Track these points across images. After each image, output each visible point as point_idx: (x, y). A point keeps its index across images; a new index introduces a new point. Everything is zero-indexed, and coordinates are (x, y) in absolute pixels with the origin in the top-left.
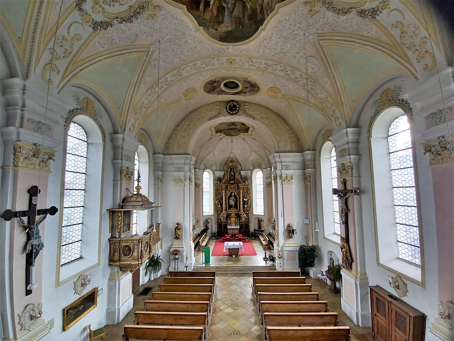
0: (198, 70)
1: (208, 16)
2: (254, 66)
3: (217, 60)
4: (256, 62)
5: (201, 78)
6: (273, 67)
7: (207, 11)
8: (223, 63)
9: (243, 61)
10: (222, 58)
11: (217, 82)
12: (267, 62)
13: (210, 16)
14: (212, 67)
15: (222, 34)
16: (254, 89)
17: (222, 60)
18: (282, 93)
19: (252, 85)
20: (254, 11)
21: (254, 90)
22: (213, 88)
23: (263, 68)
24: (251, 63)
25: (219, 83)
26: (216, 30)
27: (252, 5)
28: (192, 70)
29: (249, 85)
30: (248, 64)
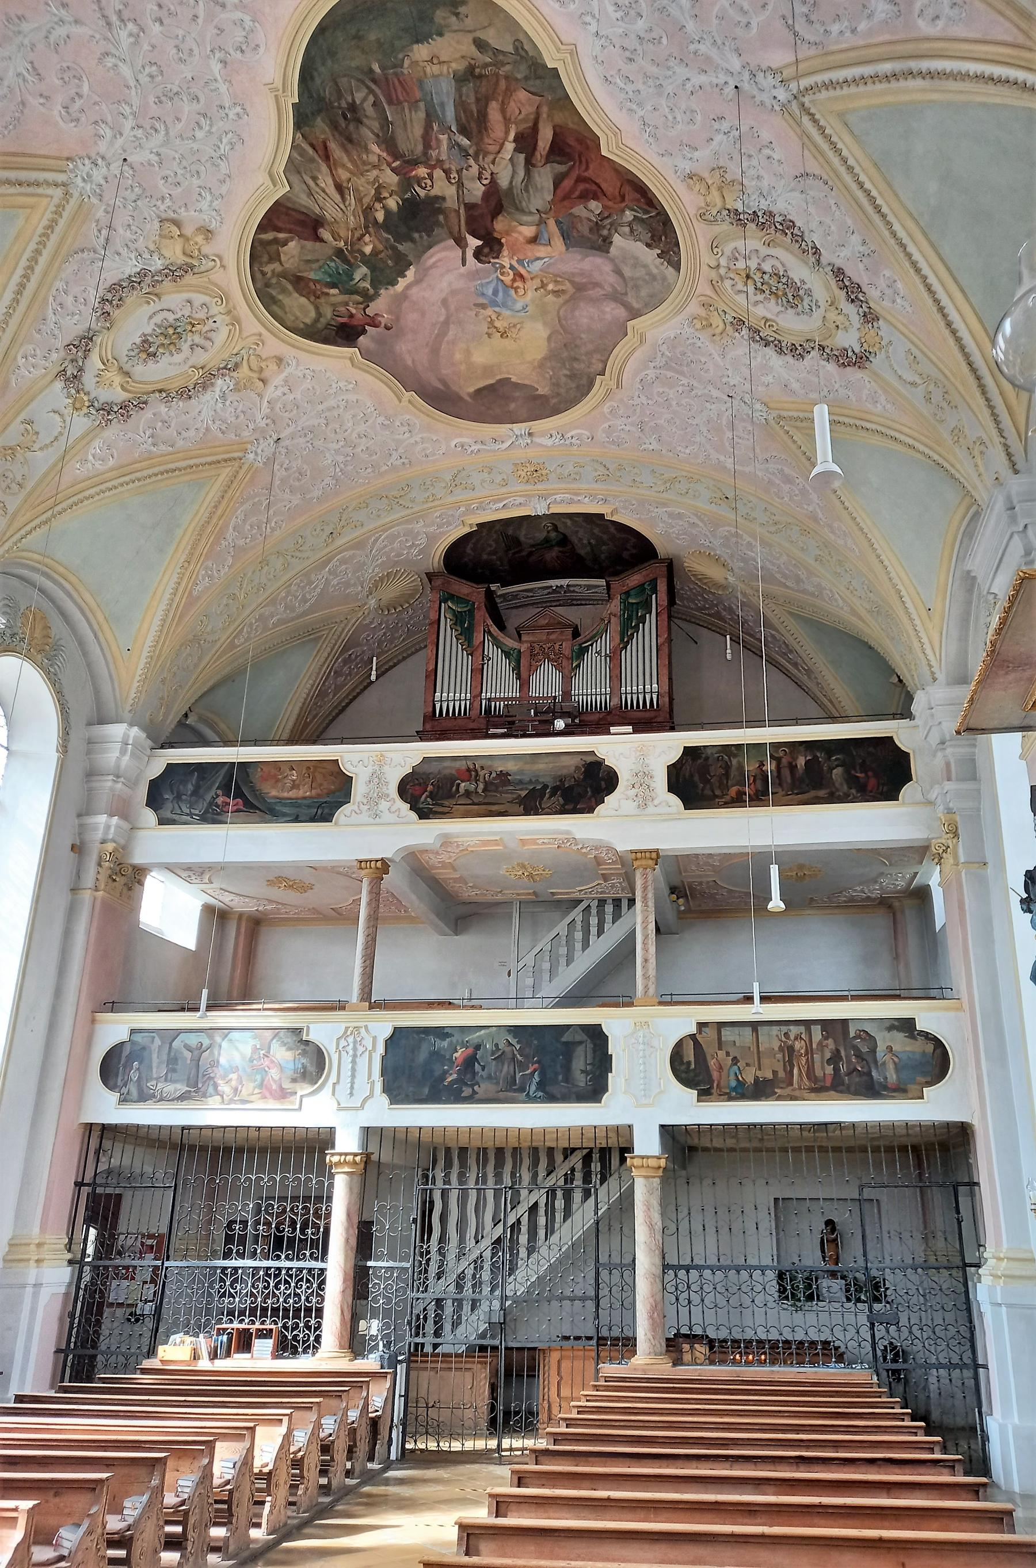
1: (523, 104)
7: (524, 120)
13: (512, 104)
20: (350, 140)
26: (480, 44)
27: (365, 157)
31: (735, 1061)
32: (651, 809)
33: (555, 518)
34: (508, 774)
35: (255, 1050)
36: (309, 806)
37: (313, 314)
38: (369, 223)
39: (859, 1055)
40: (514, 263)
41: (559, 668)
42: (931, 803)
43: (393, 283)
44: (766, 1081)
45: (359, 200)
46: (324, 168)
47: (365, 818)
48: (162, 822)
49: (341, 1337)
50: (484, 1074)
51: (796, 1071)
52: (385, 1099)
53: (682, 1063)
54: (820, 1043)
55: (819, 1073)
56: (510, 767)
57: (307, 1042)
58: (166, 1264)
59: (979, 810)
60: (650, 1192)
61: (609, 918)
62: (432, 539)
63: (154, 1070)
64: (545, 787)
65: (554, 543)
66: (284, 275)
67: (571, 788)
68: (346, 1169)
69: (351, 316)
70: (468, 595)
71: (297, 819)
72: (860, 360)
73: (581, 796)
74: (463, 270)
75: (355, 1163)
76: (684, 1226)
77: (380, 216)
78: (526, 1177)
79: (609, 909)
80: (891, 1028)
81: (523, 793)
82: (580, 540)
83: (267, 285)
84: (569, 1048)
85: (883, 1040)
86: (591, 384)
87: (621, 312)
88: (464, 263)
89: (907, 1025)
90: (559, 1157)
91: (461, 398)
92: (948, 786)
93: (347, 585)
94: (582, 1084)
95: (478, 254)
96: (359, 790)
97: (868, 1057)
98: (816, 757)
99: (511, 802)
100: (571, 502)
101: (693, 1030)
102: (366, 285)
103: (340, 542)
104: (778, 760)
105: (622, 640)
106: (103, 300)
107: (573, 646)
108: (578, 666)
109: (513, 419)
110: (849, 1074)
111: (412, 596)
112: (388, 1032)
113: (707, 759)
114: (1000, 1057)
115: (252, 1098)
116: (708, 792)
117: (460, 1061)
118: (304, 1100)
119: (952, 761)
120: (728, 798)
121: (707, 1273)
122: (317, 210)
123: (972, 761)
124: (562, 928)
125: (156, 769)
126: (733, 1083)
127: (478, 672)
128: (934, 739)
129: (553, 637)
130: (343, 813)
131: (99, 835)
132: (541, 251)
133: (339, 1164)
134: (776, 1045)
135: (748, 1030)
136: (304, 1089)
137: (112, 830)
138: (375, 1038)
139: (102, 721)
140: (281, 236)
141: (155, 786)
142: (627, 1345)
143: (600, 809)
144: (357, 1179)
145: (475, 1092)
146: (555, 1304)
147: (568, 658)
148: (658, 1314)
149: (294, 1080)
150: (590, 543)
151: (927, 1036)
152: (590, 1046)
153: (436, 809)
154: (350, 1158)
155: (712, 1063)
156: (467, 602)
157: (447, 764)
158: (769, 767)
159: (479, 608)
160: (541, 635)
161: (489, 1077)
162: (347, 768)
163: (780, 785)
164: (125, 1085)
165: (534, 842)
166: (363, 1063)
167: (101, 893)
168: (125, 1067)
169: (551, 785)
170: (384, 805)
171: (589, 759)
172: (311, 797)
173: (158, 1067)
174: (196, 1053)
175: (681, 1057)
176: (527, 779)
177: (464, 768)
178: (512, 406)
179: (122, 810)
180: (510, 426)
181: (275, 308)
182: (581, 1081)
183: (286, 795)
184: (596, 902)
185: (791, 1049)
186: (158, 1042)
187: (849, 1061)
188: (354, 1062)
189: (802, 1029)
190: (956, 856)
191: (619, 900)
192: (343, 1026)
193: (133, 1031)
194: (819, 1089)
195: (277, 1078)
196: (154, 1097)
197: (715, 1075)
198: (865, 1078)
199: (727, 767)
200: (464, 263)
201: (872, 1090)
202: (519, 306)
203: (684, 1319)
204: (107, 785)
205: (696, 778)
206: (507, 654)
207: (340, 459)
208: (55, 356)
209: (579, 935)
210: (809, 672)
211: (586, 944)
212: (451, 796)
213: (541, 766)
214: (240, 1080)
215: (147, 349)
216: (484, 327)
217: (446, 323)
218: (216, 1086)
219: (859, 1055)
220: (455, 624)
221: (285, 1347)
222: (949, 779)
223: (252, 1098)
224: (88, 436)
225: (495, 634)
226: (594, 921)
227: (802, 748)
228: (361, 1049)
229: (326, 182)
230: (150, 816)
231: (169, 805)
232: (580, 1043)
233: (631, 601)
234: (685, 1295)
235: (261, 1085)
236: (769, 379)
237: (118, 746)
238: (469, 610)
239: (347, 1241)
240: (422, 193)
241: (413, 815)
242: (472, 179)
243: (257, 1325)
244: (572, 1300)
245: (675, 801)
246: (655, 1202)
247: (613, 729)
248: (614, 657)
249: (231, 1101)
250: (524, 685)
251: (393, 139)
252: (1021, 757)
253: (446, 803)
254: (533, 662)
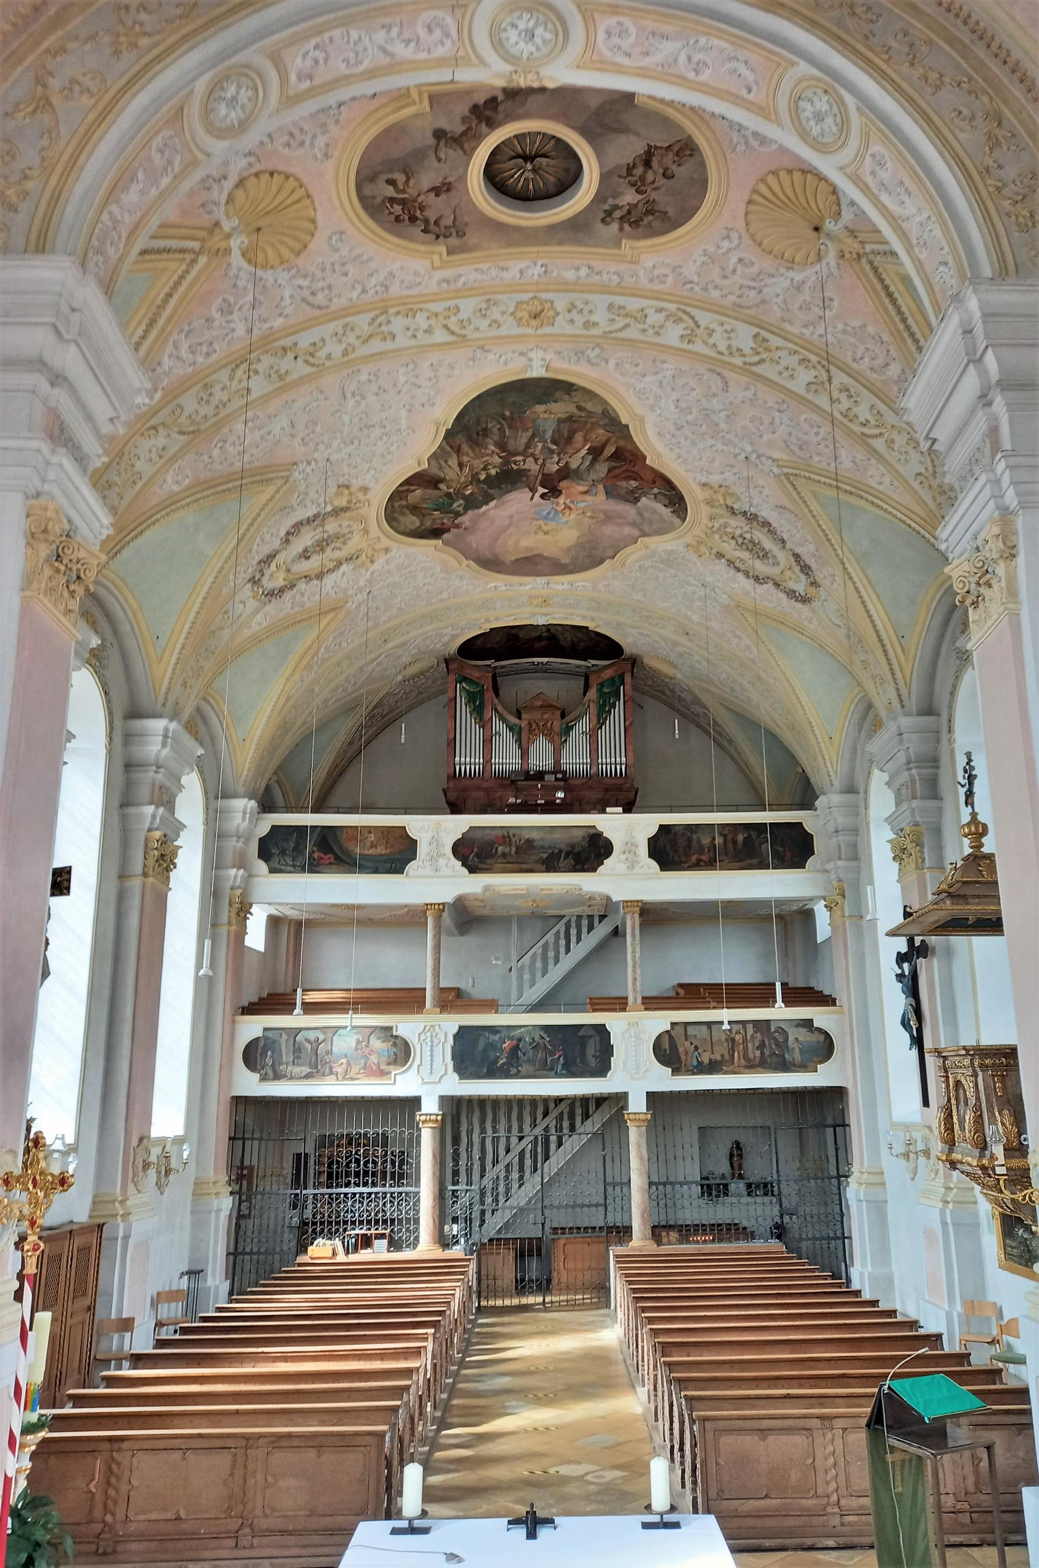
0: (684, 312)
2: (436, 315)
3: (595, 324)
4: (428, 331)
5: (690, 271)
6: (358, 337)
8: (569, 311)
9: (484, 324)
10: (569, 330)
11: (618, 214)
12: (389, 345)
14: (620, 300)
15: (566, 397)
16: (390, 191)
17: (572, 321)
18: (236, 259)
19: (413, 219)
21: (391, 182)
22: (650, 176)
23: (392, 319)
24: (453, 323)
25: (607, 207)
28: (711, 326)
29: (431, 215)
30: (463, 315)
31: (696, 1048)
32: (637, 870)
33: (548, 627)
34: (533, 841)
35: (358, 1042)
36: (385, 862)
37: (418, 524)
38: (474, 479)
39: (777, 1044)
40: (568, 502)
41: (552, 741)
42: (826, 871)
43: (479, 507)
44: (716, 1062)
45: (471, 469)
46: (455, 456)
47: (428, 871)
48: (272, 871)
49: (434, 1237)
50: (525, 1058)
51: (736, 1054)
52: (456, 1076)
53: (660, 1050)
54: (752, 1036)
55: (751, 1056)
56: (535, 835)
57: (397, 1037)
58: (304, 1192)
59: (858, 879)
60: (640, 1136)
61: (585, 929)
62: (454, 637)
63: (284, 1057)
64: (561, 851)
66: (407, 507)
67: (578, 852)
68: (431, 1125)
69: (443, 524)
70: (478, 678)
71: (376, 871)
72: (805, 600)
73: (588, 859)
74: (529, 503)
75: (437, 1120)
76: (662, 1157)
77: (482, 477)
78: (527, 1120)
79: (585, 923)
80: (797, 1026)
81: (545, 856)
83: (393, 512)
84: (584, 1041)
85: (793, 1034)
86: (602, 561)
87: (635, 532)
88: (532, 499)
89: (808, 1024)
90: (552, 1106)
91: (503, 562)
92: (840, 863)
93: (386, 670)
94: (593, 1065)
95: (543, 496)
96: (422, 850)
97: (784, 1045)
98: (750, 836)
99: (536, 862)
100: (567, 618)
101: (669, 1028)
102: (461, 509)
103: (390, 645)
104: (725, 836)
105: (599, 721)
106: (288, 533)
108: (566, 741)
109: (537, 574)
110: (770, 1056)
111: (428, 671)
112: (456, 1030)
113: (675, 834)
114: (867, 1046)
115: (358, 1076)
116: (676, 859)
117: (507, 1050)
118: (398, 1077)
119: (842, 844)
120: (690, 864)
121: (677, 1187)
122: (442, 475)
123: (855, 846)
124: (550, 937)
125: (263, 829)
126: (695, 1063)
127: (488, 742)
128: (831, 827)
129: (545, 716)
130: (411, 867)
131: (230, 883)
132: (588, 498)
133: (423, 1122)
134: (723, 1037)
135: (705, 1027)
136: (395, 1071)
137: (239, 879)
138: (446, 1034)
139: (226, 796)
140: (413, 488)
141: (262, 841)
142: (623, 1232)
143: (601, 869)
144: (438, 1131)
145: (519, 1071)
146: (578, 1209)
148: (645, 1214)
149: (389, 1064)
151: (820, 1030)
152: (598, 1039)
153: (484, 866)
154: (433, 1117)
155: (681, 1050)
156: (477, 684)
157: (487, 832)
158: (719, 840)
159: (487, 690)
160: (537, 715)
161: (529, 1061)
162: (413, 834)
163: (726, 854)
164: (263, 1068)
165: (551, 889)
166: (438, 1050)
167: (234, 927)
168: (261, 1055)
169: (565, 850)
170: (442, 862)
171: (592, 831)
172: (386, 855)
173: (287, 1056)
174: (314, 1045)
175: (660, 1046)
176: (547, 845)
177: (500, 835)
178: (539, 567)
179: (241, 863)
180: (534, 578)
181: (394, 524)
182: (592, 1062)
183: (366, 852)
184: (574, 919)
185: (733, 1040)
186: (284, 1037)
187: (771, 1047)
188: (432, 1050)
189: (741, 1026)
190: (843, 910)
191: (592, 916)
192: (422, 1025)
193: (265, 1029)
194: (751, 1066)
195: (376, 1062)
196: (285, 1076)
197: (683, 1057)
198: (781, 1059)
199: (690, 840)
200: (532, 499)
201: (784, 1066)
202: (564, 520)
203: (663, 1217)
204: (233, 844)
205: (668, 848)
206: (511, 729)
207: (407, 598)
208: (250, 570)
209: (562, 942)
210: (730, 741)
211: (568, 950)
212: (491, 856)
213: (557, 836)
214: (349, 1064)
215: (305, 555)
216: (534, 529)
217: (509, 525)
218: (331, 1068)
219: (777, 1044)
220: (469, 701)
221: (394, 1244)
222: (840, 859)
223: (358, 1076)
224: (256, 612)
226: (573, 932)
227: (741, 828)
228: (436, 1041)
229: (453, 462)
230: (262, 867)
231: (276, 859)
232: (591, 1037)
233: (606, 690)
234: (663, 1201)
235: (365, 1067)
236: (736, 586)
237: (241, 814)
239: (434, 1173)
240: (515, 467)
241: (465, 871)
242: (553, 463)
243: (373, 1231)
244: (589, 1206)
245: (654, 865)
246: (644, 1142)
247: (608, 810)
248: (593, 736)
249: (344, 1078)
250: (525, 754)
251: (506, 443)
252: (898, 881)
253: (489, 861)
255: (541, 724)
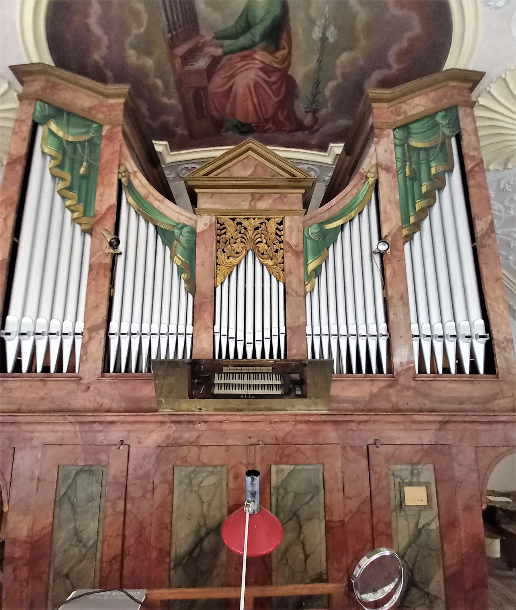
65: (258, 31)
70: (90, 109)
82: (312, 22)
107: (306, 226)
108: (317, 272)
129: (263, 205)
147: (297, 253)
150: (324, 39)
225: (142, 191)
233: (414, 143)
238: (90, 141)
254: (222, 257)
255: (251, 224)
